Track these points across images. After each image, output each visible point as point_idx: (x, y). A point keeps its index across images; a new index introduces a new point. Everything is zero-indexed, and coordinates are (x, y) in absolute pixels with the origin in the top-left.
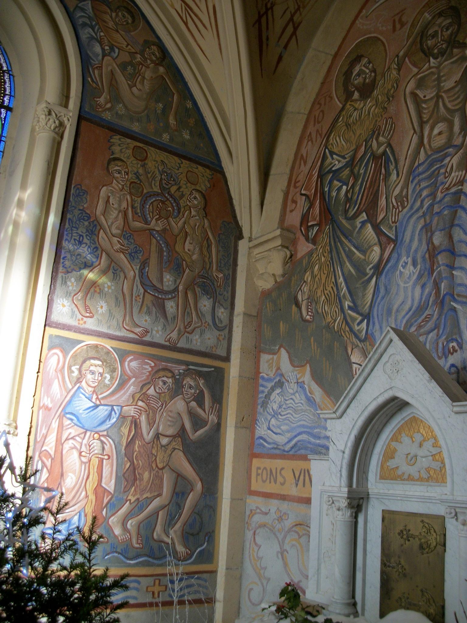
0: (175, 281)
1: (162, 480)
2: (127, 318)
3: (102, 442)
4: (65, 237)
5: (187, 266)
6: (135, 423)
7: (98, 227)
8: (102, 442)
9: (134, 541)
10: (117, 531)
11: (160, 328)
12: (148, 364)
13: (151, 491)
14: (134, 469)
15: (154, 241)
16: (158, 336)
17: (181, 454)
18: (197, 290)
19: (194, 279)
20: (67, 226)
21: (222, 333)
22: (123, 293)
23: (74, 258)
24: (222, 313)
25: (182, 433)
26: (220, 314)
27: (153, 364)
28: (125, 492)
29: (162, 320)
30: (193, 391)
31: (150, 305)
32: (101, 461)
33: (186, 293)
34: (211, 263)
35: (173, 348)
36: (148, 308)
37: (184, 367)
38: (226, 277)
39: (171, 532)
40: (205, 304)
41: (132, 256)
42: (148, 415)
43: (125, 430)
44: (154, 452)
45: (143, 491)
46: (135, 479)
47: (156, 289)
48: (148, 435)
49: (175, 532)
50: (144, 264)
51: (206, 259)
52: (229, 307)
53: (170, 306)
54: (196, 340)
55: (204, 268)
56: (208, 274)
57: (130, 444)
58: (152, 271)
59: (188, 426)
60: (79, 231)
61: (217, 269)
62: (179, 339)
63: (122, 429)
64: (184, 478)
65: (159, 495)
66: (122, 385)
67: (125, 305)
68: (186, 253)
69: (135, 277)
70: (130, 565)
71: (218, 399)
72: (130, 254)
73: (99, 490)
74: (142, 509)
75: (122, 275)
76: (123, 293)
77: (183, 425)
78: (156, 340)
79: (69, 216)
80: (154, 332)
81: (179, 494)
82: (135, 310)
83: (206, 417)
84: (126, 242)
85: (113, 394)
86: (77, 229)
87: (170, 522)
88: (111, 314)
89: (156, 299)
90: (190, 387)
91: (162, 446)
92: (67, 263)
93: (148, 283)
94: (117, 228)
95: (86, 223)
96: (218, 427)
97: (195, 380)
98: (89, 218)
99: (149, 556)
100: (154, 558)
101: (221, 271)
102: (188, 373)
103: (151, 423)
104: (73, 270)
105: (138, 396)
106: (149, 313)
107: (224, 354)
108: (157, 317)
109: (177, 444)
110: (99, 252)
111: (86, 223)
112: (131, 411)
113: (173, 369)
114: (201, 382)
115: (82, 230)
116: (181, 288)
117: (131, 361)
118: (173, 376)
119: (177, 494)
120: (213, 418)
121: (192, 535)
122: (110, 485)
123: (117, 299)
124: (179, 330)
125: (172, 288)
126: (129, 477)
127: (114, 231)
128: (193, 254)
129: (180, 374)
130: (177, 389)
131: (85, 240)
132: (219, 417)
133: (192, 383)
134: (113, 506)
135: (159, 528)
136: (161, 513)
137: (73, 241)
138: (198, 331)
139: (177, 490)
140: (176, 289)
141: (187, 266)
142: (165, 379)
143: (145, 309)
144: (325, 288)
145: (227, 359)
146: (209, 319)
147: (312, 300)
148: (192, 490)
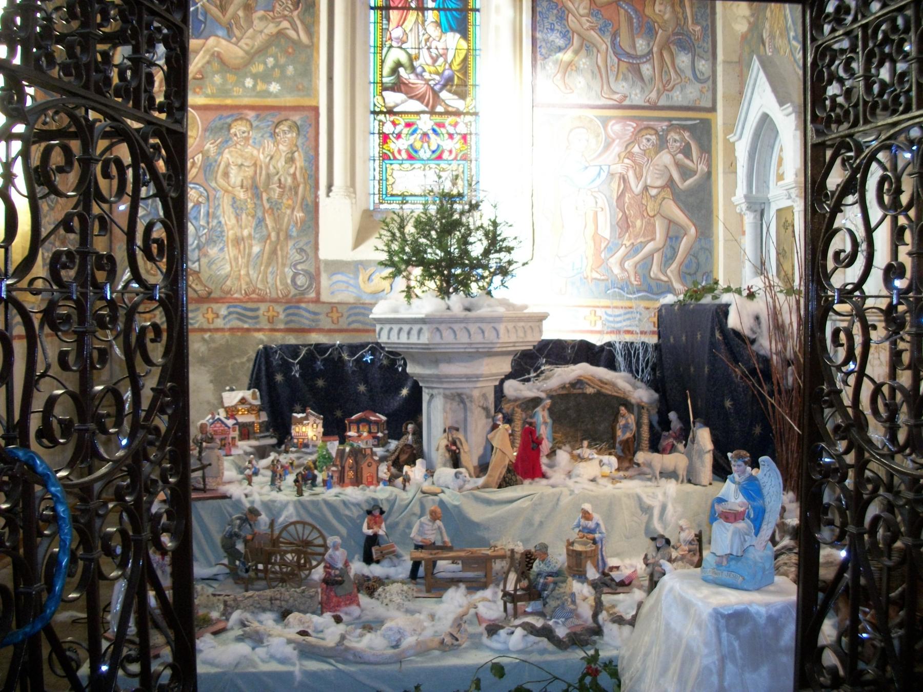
0: (649, 44)
1: (654, 226)
2: (605, 88)
3: (595, 197)
4: (538, 28)
5: (660, 27)
6: (624, 179)
7: (566, 12)
8: (595, 197)
9: (632, 279)
10: (617, 270)
11: (638, 91)
12: (630, 125)
13: (644, 236)
14: (627, 218)
15: (622, 11)
16: (637, 98)
17: (672, 202)
18: (673, 48)
19: (669, 38)
20: (538, 18)
21: (706, 85)
22: (598, 66)
23: (549, 45)
24: (703, 66)
25: (671, 183)
26: (701, 67)
27: (635, 125)
28: (620, 238)
29: (639, 83)
30: (678, 144)
31: (625, 71)
32: (596, 213)
33: (661, 54)
34: (686, 18)
35: (654, 107)
36: (624, 75)
37: (666, 123)
38: (704, 29)
39: (668, 272)
40: (684, 60)
41: (602, 31)
42: (635, 170)
43: (614, 185)
44: (644, 202)
45: (637, 237)
46: (628, 227)
47: (629, 55)
48: (637, 188)
49: (671, 271)
50: (615, 35)
51: (680, 16)
52: (711, 58)
53: (646, 69)
54: (677, 96)
55: (678, 24)
56: (683, 29)
57: (621, 197)
58: (624, 40)
59: (676, 176)
60: (550, 21)
61: (693, 23)
62: (658, 99)
63: (612, 184)
64: (676, 224)
65: (653, 239)
66: (608, 146)
67: (601, 77)
68: (656, 14)
69: (607, 49)
70: (630, 299)
71: (706, 149)
72: (600, 29)
73: (596, 237)
74: (637, 251)
75: (595, 50)
76: (598, 66)
77: (671, 177)
78: (635, 103)
79: (538, 9)
80: (633, 96)
81: (673, 235)
82: (612, 79)
83: (695, 167)
84: (594, 19)
85: (600, 155)
86: (547, 18)
87: (667, 261)
88: (589, 86)
89: (632, 66)
90: (675, 141)
91: (651, 197)
92: (544, 51)
93: (621, 52)
94: (585, 8)
95: (555, 11)
96: (709, 175)
97: (680, 133)
98: (557, 6)
99: (647, 292)
100: (653, 294)
101: (697, 24)
102: (671, 128)
103: (638, 177)
104: (550, 55)
105: (623, 155)
106: (625, 79)
107: (709, 105)
108: (634, 82)
109: (667, 193)
110: (570, 34)
111: (555, 11)
112: (618, 168)
113: (655, 127)
114: (686, 135)
115: (552, 19)
116: (655, 49)
117: (613, 125)
118: (657, 133)
119: (671, 238)
120: (702, 168)
121: (690, 274)
122: (606, 231)
123: (593, 73)
124: (658, 90)
125: (646, 51)
126: (624, 225)
127: (582, 11)
128: (665, 13)
129: (663, 130)
130: (662, 143)
131: (557, 27)
132: (709, 166)
133: (677, 137)
134: (611, 249)
135: (655, 268)
136: (656, 256)
137: (545, 31)
138: (678, 87)
139: (671, 234)
140: (651, 52)
141: (660, 27)
142: (648, 136)
143: (621, 76)
144: (779, 23)
145: (713, 109)
146: (689, 73)
147: (772, 36)
148: (685, 234)
